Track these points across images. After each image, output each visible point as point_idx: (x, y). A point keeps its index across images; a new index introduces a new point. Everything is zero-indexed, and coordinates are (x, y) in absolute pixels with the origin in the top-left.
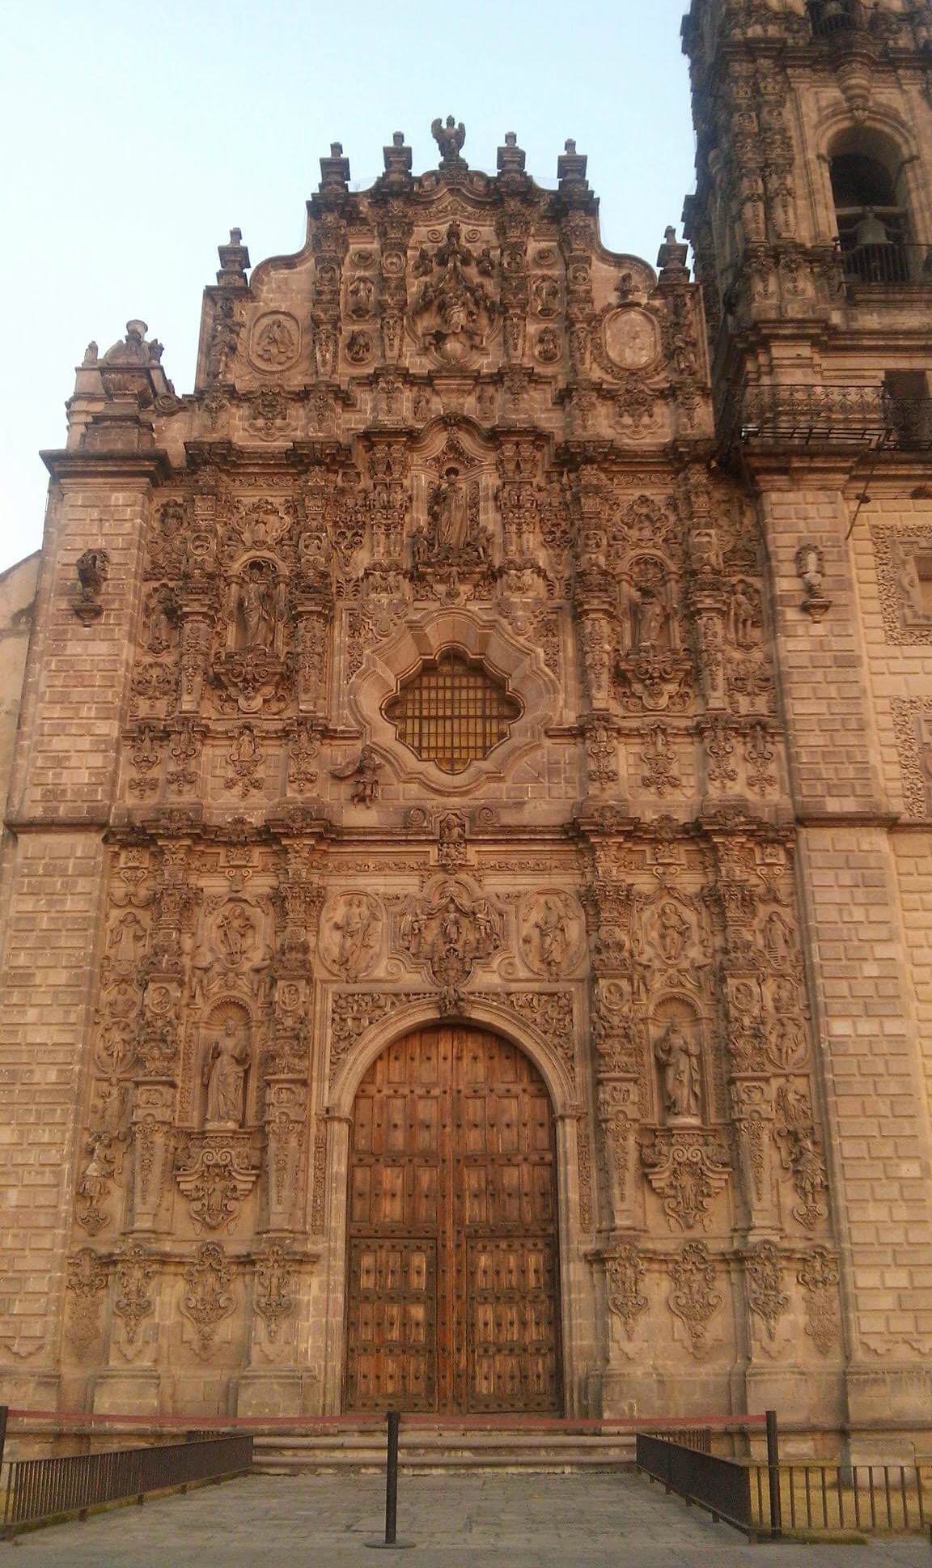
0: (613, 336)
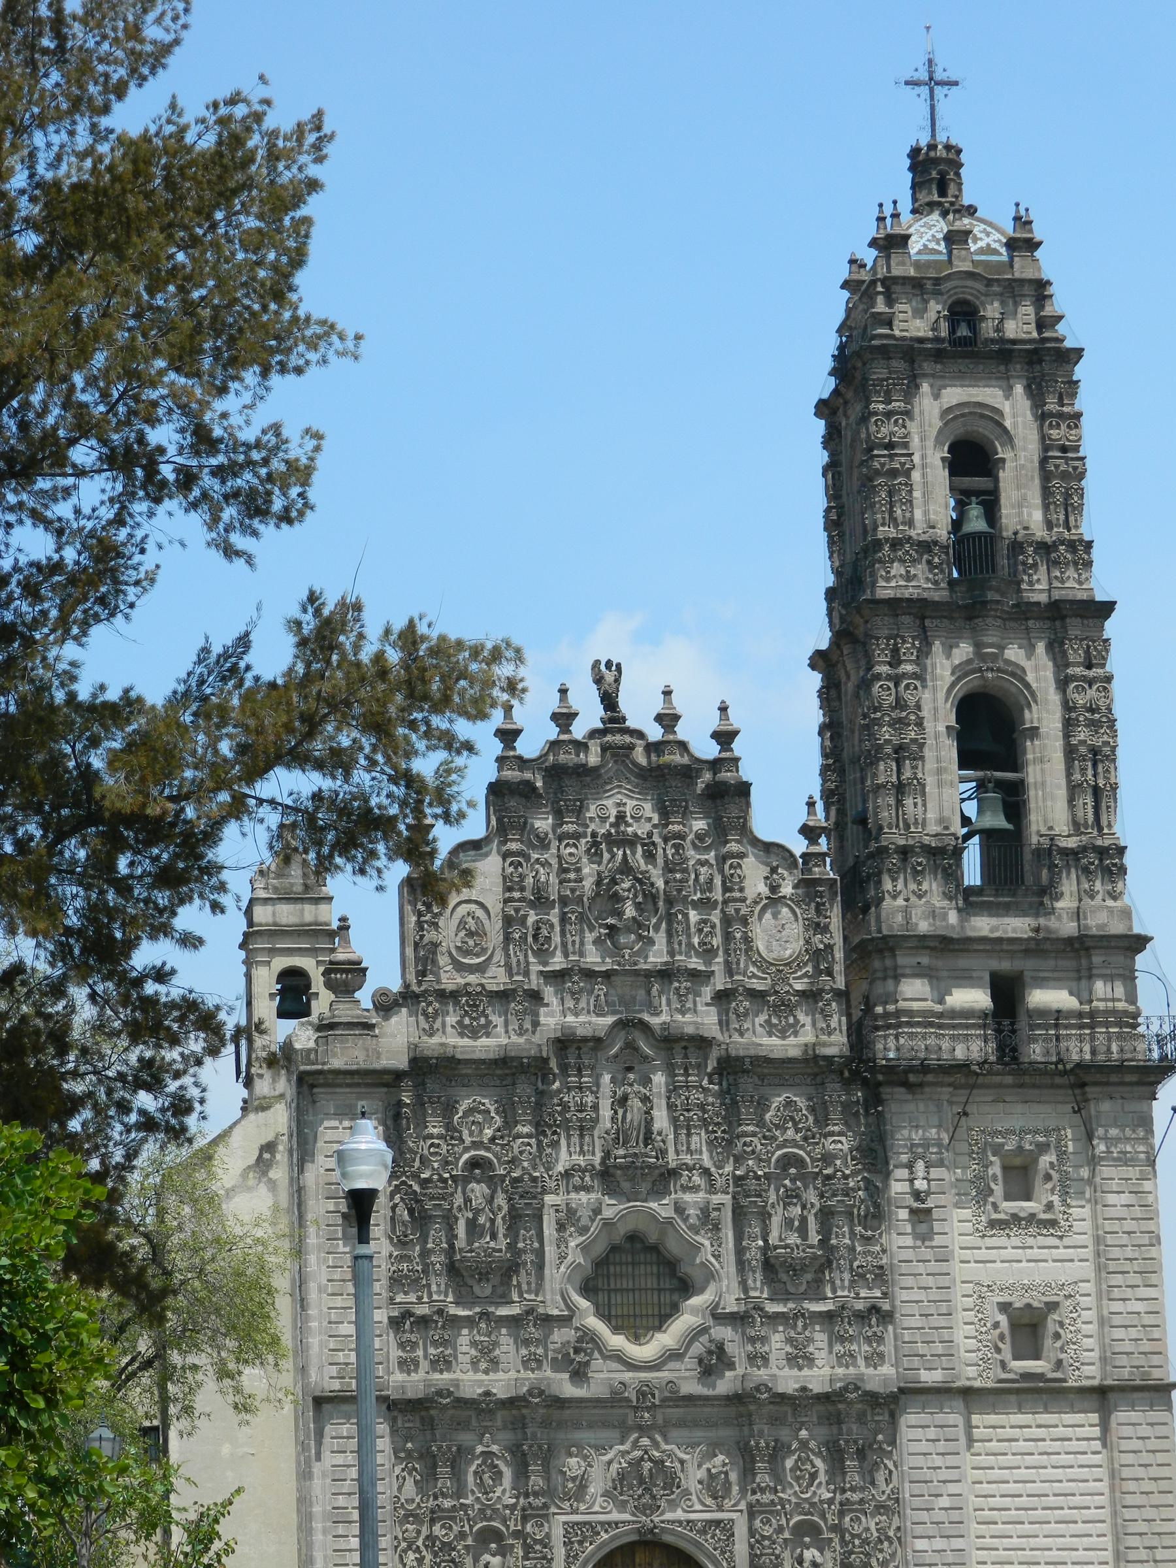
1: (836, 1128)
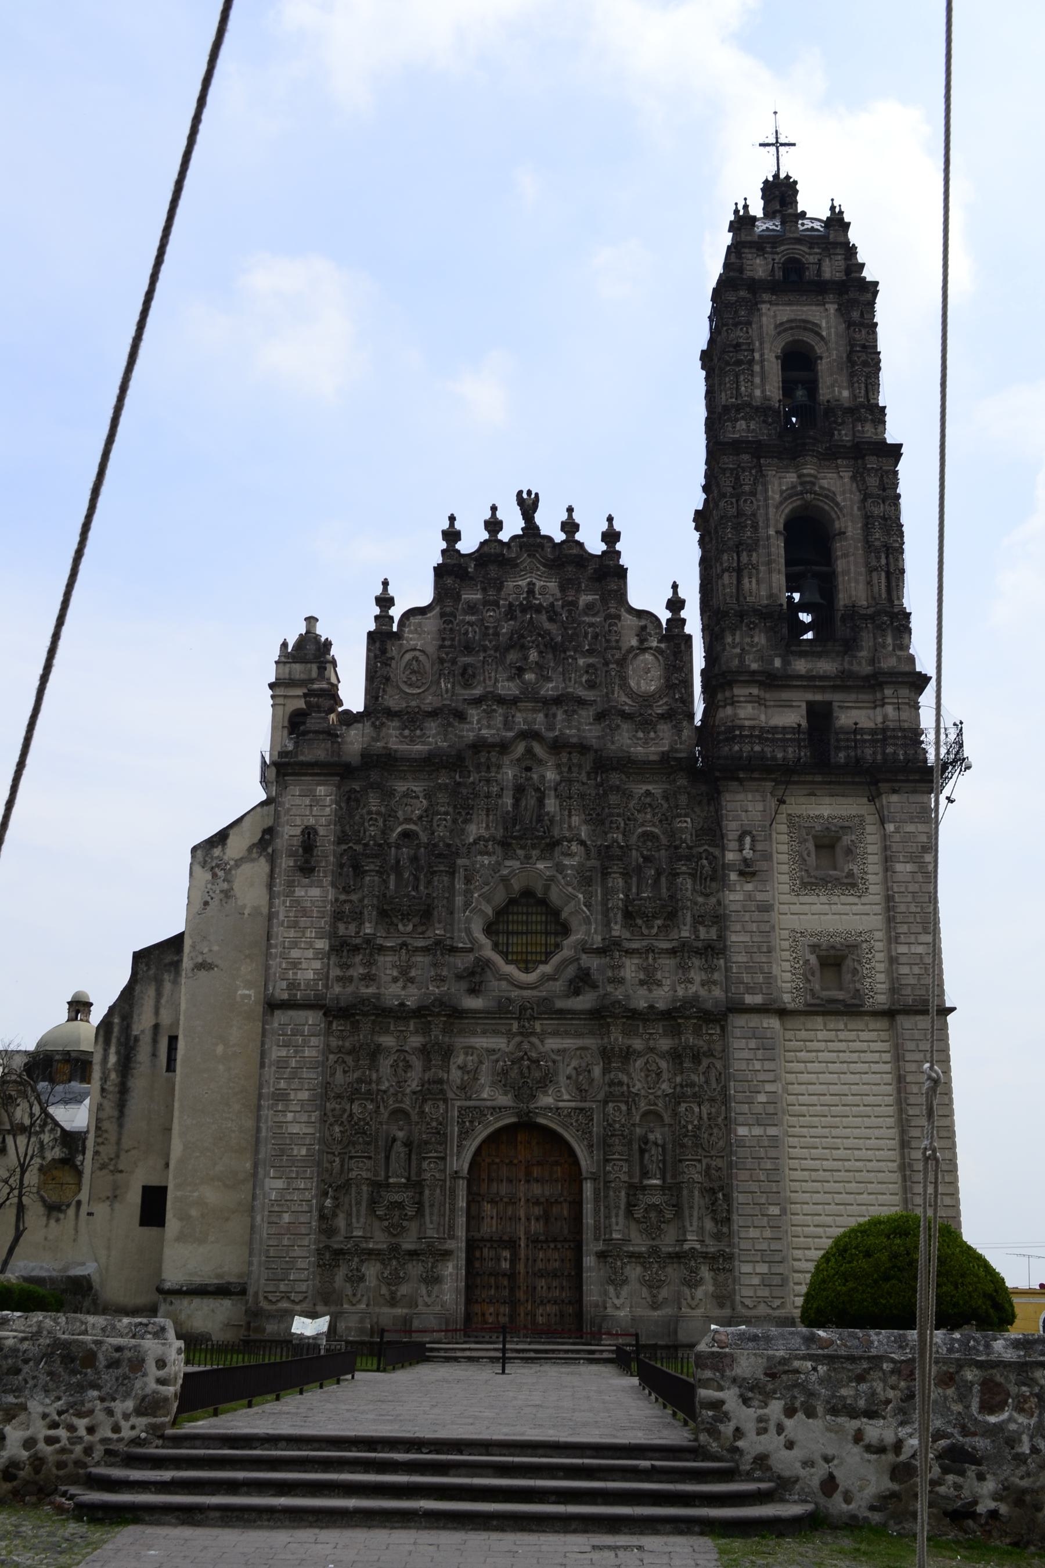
0: (633, 670)
1: (683, 811)
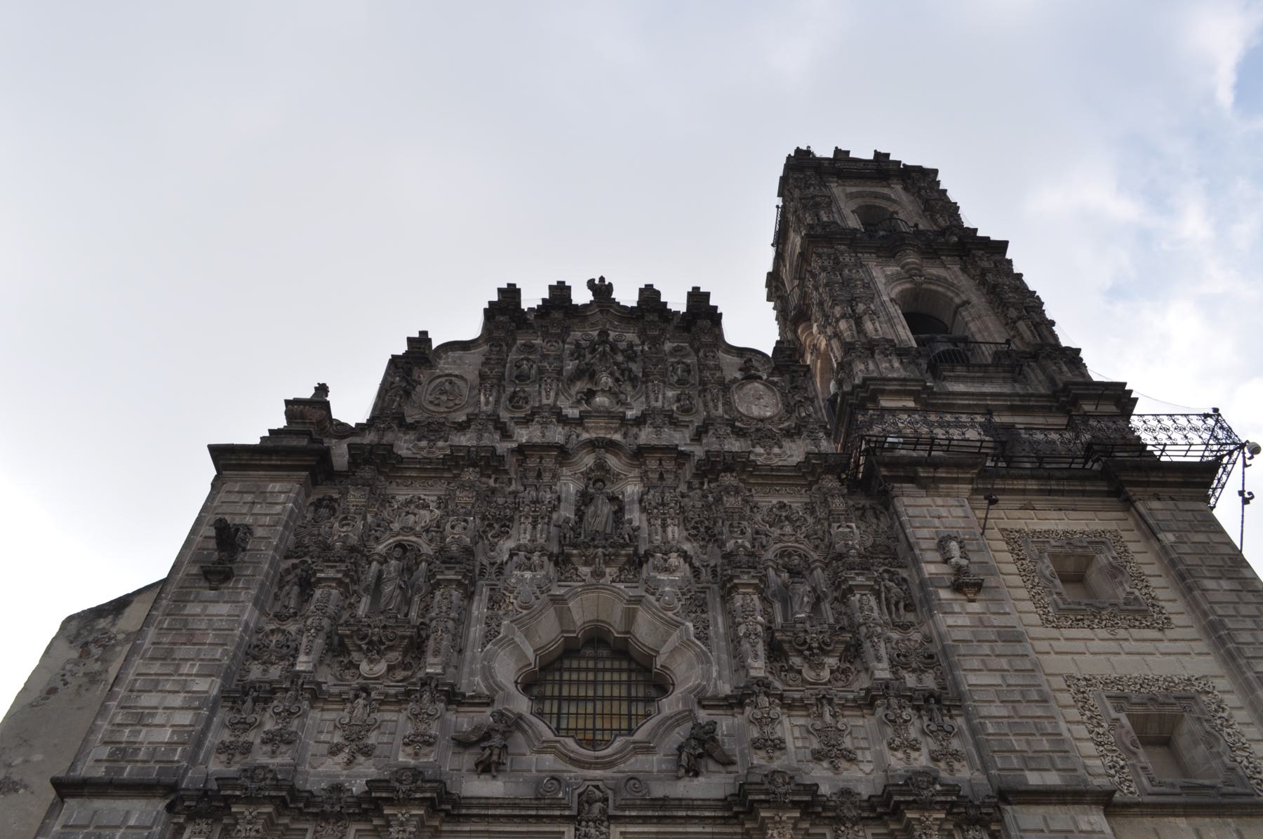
0: (740, 398)
